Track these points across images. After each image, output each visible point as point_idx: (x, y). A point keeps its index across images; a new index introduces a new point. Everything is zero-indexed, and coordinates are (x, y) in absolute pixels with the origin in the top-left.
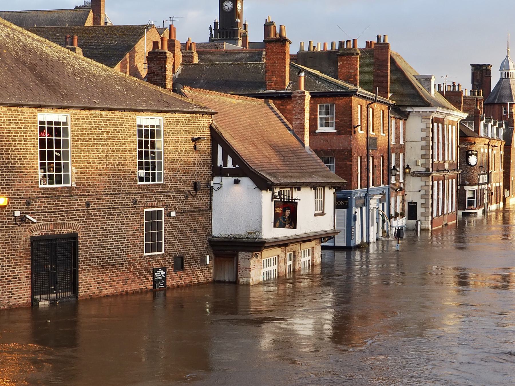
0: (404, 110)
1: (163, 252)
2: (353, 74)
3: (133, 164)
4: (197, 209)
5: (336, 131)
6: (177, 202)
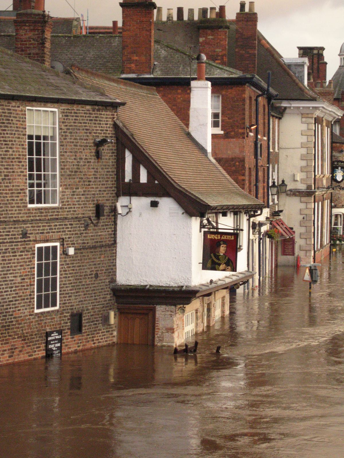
0: (278, 105)
1: (57, 308)
2: (220, 54)
3: (22, 177)
4: (99, 244)
5: (222, 132)
6: (76, 234)
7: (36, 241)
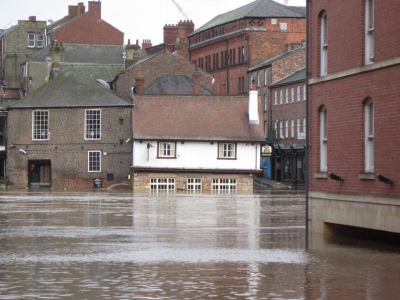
7: (89, 150)
